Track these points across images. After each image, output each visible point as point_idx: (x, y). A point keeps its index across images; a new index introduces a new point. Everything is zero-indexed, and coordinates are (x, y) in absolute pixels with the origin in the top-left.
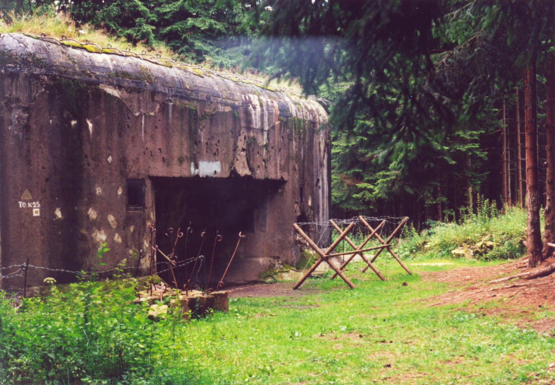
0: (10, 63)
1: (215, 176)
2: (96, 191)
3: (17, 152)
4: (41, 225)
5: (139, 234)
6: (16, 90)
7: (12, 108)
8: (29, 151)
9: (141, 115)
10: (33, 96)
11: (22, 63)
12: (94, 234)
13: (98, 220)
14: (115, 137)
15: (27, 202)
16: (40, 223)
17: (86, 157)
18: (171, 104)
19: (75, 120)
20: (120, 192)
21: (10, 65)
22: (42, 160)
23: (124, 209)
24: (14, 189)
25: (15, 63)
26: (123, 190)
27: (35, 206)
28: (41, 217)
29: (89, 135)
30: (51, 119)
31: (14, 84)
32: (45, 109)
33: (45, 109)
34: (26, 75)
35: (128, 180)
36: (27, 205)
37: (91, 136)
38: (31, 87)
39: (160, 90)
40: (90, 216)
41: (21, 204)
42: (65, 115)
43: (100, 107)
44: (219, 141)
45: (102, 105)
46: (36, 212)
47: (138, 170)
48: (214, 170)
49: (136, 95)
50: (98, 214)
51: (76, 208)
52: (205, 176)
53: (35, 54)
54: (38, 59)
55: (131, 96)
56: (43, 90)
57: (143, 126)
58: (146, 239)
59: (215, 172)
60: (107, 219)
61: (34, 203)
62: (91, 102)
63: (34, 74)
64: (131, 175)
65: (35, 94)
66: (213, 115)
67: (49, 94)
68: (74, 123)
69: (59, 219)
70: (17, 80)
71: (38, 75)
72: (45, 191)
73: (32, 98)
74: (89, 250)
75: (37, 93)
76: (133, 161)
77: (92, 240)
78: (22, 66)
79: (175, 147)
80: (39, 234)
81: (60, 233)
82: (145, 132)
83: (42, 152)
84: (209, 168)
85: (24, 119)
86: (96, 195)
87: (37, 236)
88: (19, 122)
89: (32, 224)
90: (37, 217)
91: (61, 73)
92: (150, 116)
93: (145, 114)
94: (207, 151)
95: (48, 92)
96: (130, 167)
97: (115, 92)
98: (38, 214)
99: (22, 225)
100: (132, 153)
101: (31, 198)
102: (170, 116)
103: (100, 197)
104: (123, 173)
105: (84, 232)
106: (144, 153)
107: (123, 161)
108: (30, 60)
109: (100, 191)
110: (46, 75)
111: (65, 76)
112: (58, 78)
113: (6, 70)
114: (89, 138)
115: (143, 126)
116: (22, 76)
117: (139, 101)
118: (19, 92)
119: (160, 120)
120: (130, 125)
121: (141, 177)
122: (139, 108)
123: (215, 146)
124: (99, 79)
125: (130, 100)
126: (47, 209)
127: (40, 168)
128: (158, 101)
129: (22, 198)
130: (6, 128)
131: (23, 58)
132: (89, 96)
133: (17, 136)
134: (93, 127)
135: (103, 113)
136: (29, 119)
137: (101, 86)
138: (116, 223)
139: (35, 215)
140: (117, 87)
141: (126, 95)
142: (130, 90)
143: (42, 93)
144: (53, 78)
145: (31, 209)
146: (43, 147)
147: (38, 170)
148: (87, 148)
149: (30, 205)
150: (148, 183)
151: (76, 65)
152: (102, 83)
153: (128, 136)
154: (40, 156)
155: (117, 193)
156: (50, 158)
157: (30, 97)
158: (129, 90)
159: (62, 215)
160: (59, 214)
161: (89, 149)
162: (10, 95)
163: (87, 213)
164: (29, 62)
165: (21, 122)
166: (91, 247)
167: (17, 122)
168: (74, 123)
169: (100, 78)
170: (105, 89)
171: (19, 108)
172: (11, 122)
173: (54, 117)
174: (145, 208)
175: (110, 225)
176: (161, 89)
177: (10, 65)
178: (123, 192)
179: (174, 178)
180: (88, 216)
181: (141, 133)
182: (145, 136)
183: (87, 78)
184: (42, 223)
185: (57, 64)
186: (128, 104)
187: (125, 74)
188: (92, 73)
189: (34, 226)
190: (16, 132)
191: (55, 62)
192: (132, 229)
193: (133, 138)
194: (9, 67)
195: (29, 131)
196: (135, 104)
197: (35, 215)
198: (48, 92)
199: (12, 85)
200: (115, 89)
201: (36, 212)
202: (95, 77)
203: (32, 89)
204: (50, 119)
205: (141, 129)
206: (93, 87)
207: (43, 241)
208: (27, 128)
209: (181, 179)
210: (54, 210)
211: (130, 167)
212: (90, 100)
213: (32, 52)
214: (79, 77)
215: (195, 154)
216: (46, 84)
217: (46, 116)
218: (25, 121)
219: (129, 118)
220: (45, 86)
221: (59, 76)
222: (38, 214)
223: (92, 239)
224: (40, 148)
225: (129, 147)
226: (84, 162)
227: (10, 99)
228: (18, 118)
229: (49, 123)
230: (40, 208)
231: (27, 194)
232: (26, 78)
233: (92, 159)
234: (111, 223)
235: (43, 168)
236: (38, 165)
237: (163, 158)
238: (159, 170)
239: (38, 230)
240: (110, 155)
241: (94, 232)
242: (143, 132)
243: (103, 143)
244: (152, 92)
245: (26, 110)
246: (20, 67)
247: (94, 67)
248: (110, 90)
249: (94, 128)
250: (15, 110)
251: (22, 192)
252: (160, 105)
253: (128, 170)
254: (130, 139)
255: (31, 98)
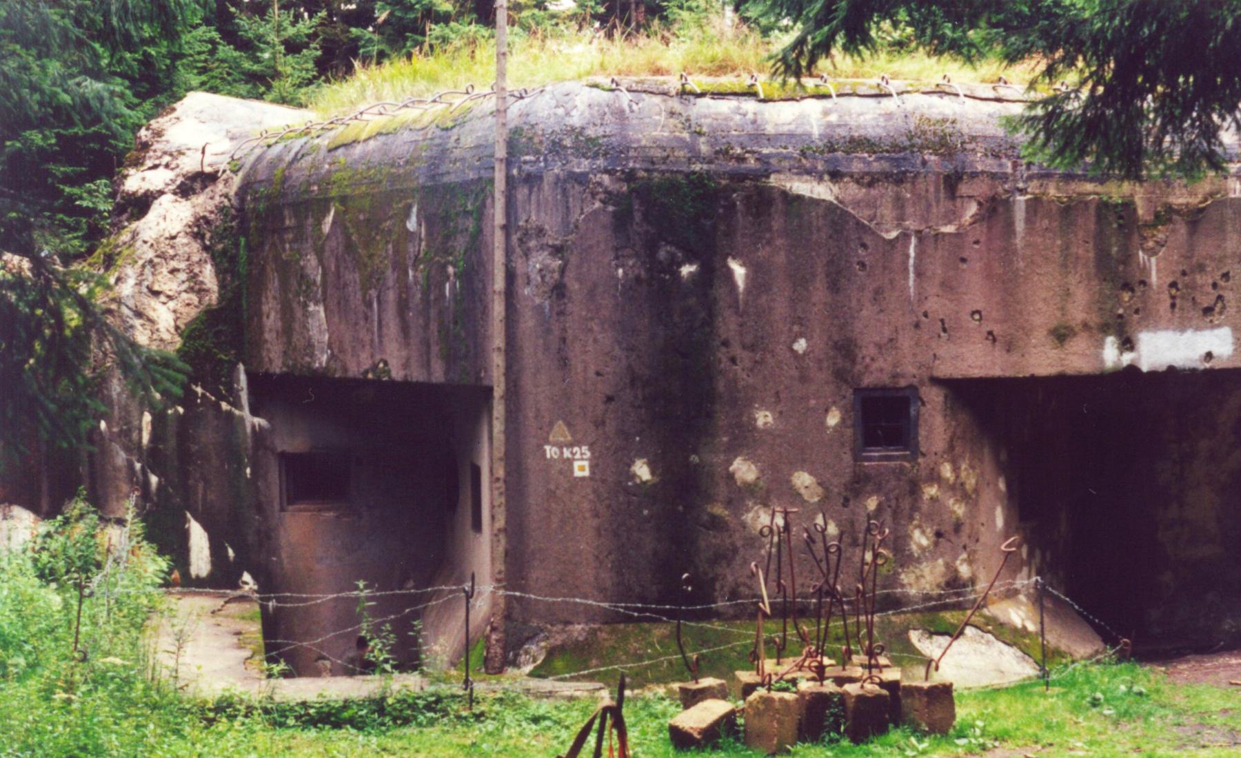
0: (527, 154)
1: (1208, 365)
2: (755, 420)
3: (541, 341)
4: (591, 497)
5: (896, 515)
6: (538, 211)
7: (529, 249)
8: (564, 340)
9: (905, 236)
10: (573, 220)
11: (550, 152)
12: (751, 515)
13: (761, 483)
14: (819, 293)
15: (561, 446)
16: (589, 490)
17: (726, 343)
18: (1021, 199)
19: (691, 263)
20: (833, 419)
21: (527, 158)
22: (597, 353)
23: (847, 458)
24: (536, 417)
25: (537, 152)
26: (845, 412)
27: (578, 456)
28: (591, 478)
29: (737, 295)
30: (623, 266)
31: (533, 198)
32: (602, 246)
33: (602, 246)
34: (557, 176)
35: (857, 391)
36: (562, 453)
37: (741, 297)
38: (567, 202)
39: (980, 168)
40: (737, 476)
41: (551, 451)
42: (662, 254)
43: (770, 229)
44: (1226, 276)
45: (777, 224)
46: (581, 468)
47: (895, 366)
48: (1203, 351)
49: (890, 190)
50: (762, 471)
51: (694, 458)
52: (1164, 368)
53: (583, 128)
54: (589, 139)
55: (873, 192)
56: (597, 205)
57: (911, 261)
58: (919, 527)
59: (1209, 356)
60: (789, 481)
61: (576, 449)
62: (741, 220)
63: (574, 173)
64: (867, 381)
65: (576, 216)
66: (1201, 210)
67: (614, 213)
68: (687, 270)
69: (645, 483)
70: (539, 189)
71: (585, 175)
72: (603, 423)
73: (572, 226)
74: (735, 550)
75: (582, 213)
76: (879, 346)
77: (744, 527)
78: (550, 158)
79: (1040, 305)
80: (588, 515)
81: (646, 512)
82: (919, 274)
83: (595, 341)
84: (1165, 348)
85: (554, 271)
86: (755, 428)
87: (585, 518)
88: (543, 277)
89: (571, 492)
90: (583, 479)
91: (653, 163)
92: (938, 236)
93: (918, 232)
94: (1173, 306)
95: (611, 208)
96: (868, 360)
97: (822, 191)
98: (586, 473)
99: (551, 494)
100: (870, 327)
101: (569, 438)
102: (1020, 226)
103: (766, 431)
104: (841, 376)
105: (718, 510)
106: (917, 326)
107: (845, 348)
108: (568, 142)
109: (770, 419)
110: (606, 171)
111: (663, 167)
112: (642, 174)
113: (520, 168)
114: (737, 301)
115: (911, 261)
116: (548, 178)
117: (899, 202)
118: (542, 214)
119: (977, 242)
120: (867, 261)
121: (903, 383)
122: (901, 218)
123: (1210, 289)
124: (768, 163)
125: (872, 204)
126: (612, 460)
127: (591, 374)
128: (970, 197)
129: (551, 438)
130: (520, 291)
131: (553, 142)
132: (734, 205)
133: (539, 309)
134: (747, 276)
135: (779, 242)
136: (563, 270)
137: (774, 180)
138: (820, 490)
139: (578, 473)
140: (826, 177)
141: (853, 191)
142: (870, 180)
143: (595, 212)
144: (630, 176)
145: (570, 462)
146: (595, 328)
147: (586, 379)
148: (728, 325)
149: (567, 453)
150: (934, 397)
151: (703, 139)
152: (778, 172)
153: (862, 288)
154: (590, 348)
155: (823, 423)
156: (617, 351)
157: (565, 222)
158: (867, 179)
159: (653, 473)
160: (642, 471)
161: (733, 326)
162: (527, 221)
163: (727, 469)
164: (565, 147)
165: (547, 279)
166: (739, 543)
167: (539, 279)
168: (687, 270)
169: (773, 161)
170: (788, 185)
171: (542, 248)
172: (528, 278)
173: (631, 263)
174: (916, 452)
175: (799, 495)
176: (980, 162)
177: (527, 158)
178: (843, 420)
179: (1033, 378)
180: (731, 476)
181: (906, 278)
182: (918, 285)
183: (732, 164)
184: (595, 491)
185: (643, 143)
186: (862, 215)
187: (858, 144)
188: (748, 152)
189: (576, 498)
190: (538, 301)
191: (639, 141)
192: (872, 504)
193: (878, 292)
194: (525, 162)
195: (563, 296)
196: (886, 212)
197: (578, 473)
198: (611, 208)
199: (530, 200)
200: (821, 180)
201: (582, 468)
202: (757, 160)
203: (571, 205)
204: (617, 267)
205: (906, 269)
206: (748, 183)
207: (598, 530)
208: (559, 290)
209: (1063, 384)
210: (630, 463)
211: (868, 360)
212: (739, 215)
213: (578, 125)
214: (705, 167)
215: (1120, 316)
216: (606, 192)
217: (606, 261)
218: (556, 276)
219: (864, 246)
220: (602, 196)
221: (646, 170)
222: (586, 473)
223: (744, 526)
224: (591, 330)
225: (864, 313)
226: (720, 355)
227: (526, 230)
228: (541, 270)
229: (615, 278)
230: (590, 460)
231: (560, 431)
232: (556, 184)
233: (744, 347)
234: (803, 491)
235: (598, 374)
236: (585, 369)
237: (990, 333)
238: (975, 360)
239: (586, 505)
240: (801, 335)
241: (748, 511)
242: (912, 275)
243: (781, 307)
244: (947, 178)
245: (557, 251)
246: (545, 160)
247: (759, 136)
248: (803, 187)
249: (751, 279)
250: (534, 254)
251: (551, 424)
252: (980, 204)
253: (859, 367)
254: (869, 294)
255: (568, 224)
